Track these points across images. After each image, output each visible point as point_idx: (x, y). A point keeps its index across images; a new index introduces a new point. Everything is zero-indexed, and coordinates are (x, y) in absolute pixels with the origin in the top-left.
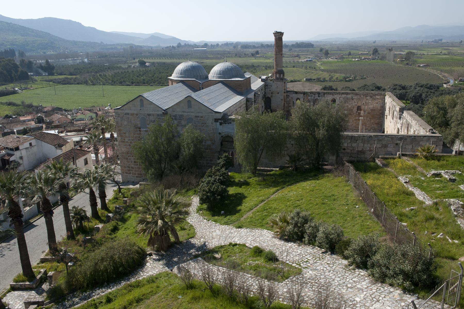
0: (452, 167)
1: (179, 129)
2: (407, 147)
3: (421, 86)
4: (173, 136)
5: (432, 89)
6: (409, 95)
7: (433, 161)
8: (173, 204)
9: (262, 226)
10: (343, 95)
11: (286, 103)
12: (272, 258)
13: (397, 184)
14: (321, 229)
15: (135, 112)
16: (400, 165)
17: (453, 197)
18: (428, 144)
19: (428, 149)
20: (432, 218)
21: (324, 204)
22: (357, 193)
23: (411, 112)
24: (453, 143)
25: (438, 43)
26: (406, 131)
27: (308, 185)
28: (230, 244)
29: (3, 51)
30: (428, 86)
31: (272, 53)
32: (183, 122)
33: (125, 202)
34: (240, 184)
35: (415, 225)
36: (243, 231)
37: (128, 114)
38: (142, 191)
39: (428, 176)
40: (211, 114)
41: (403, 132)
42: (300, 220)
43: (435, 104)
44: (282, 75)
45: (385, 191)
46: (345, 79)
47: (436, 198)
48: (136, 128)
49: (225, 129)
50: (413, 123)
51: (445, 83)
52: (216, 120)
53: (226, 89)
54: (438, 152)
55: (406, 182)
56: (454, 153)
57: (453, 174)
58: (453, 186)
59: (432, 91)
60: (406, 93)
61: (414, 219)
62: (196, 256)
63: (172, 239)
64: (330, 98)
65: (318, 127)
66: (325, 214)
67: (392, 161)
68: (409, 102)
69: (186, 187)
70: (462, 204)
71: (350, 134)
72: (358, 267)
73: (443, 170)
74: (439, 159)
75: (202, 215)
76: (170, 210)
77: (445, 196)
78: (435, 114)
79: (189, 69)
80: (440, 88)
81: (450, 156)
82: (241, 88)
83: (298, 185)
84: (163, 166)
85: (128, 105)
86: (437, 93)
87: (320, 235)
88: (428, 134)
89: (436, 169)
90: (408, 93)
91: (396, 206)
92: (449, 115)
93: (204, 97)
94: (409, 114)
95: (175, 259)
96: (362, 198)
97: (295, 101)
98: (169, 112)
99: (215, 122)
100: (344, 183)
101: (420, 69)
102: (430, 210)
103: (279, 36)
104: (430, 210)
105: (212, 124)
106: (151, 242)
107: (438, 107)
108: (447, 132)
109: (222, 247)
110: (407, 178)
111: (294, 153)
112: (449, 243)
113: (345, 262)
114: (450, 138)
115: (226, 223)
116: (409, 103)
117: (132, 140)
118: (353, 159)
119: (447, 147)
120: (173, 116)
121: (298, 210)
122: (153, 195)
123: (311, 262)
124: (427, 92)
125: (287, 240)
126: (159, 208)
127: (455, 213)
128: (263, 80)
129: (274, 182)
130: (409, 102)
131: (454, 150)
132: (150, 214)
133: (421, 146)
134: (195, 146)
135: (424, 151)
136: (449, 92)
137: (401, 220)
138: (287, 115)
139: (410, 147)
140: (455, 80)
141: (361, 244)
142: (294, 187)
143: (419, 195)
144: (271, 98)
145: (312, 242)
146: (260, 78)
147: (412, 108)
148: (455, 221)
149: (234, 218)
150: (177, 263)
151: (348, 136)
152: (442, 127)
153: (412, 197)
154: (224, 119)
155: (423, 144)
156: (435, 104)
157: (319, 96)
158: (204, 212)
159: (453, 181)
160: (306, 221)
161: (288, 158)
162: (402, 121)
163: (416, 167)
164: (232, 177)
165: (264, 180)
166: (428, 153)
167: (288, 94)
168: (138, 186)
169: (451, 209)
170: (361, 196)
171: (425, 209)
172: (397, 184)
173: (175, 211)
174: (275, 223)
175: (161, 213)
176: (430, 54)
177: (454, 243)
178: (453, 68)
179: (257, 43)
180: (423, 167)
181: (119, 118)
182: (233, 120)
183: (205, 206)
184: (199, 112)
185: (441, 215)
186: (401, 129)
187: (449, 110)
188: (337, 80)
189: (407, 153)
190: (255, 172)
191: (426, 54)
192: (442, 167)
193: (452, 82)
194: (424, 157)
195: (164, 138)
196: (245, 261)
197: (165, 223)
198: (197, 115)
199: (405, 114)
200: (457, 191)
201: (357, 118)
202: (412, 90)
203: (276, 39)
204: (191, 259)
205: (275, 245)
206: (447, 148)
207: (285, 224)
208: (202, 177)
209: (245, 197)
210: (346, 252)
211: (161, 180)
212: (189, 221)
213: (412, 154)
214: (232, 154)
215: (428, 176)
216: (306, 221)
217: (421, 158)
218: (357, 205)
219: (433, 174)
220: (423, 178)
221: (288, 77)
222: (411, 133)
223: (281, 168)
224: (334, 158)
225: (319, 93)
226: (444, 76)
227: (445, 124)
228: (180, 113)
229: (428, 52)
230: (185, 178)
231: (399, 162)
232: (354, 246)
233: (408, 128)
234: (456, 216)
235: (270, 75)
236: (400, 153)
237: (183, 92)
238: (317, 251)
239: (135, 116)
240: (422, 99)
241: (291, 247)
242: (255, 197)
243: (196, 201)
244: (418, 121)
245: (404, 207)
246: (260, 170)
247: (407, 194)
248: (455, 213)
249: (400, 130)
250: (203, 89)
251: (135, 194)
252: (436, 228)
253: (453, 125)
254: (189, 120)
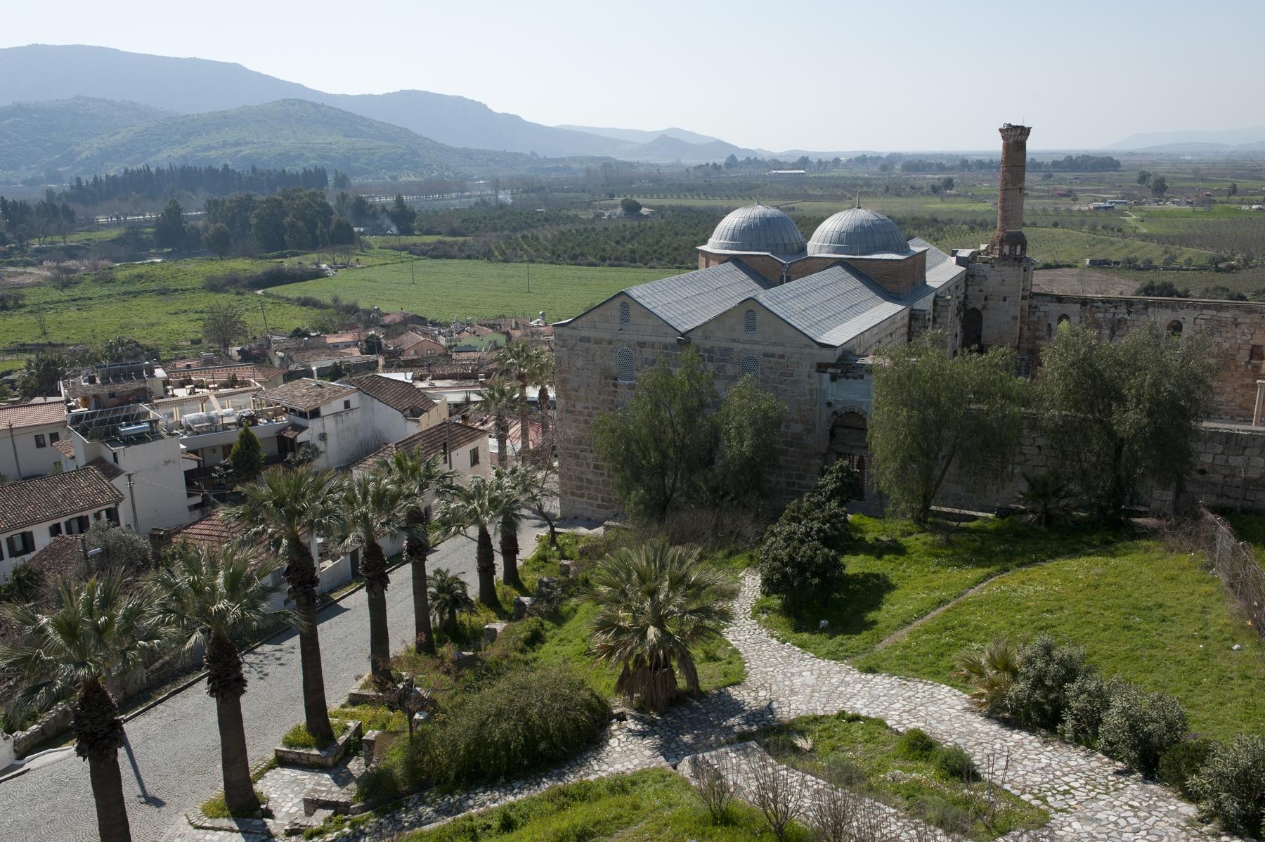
1: (719, 385)
4: (702, 404)
8: (689, 587)
9: (936, 675)
10: (1205, 312)
11: (1025, 328)
12: (961, 769)
14: (1117, 703)
15: (607, 336)
21: (1128, 628)
22: (1237, 605)
27: (1080, 569)
28: (842, 714)
29: (301, 172)
31: (993, 184)
32: (730, 369)
33: (565, 571)
34: (878, 550)
36: (880, 682)
37: (588, 340)
38: (610, 546)
40: (808, 350)
42: (1053, 668)
44: (1019, 248)
46: (1214, 265)
48: (606, 378)
49: (845, 394)
52: (821, 368)
53: (854, 283)
62: (744, 737)
63: (682, 683)
64: (1163, 318)
65: (1122, 400)
66: (1131, 658)
69: (728, 545)
71: (1223, 426)
72: (1231, 830)
75: (766, 624)
76: (679, 600)
79: (756, 225)
82: (897, 282)
83: (1051, 565)
84: (669, 481)
85: (589, 316)
87: (1112, 719)
93: (790, 302)
95: (687, 738)
96: (1254, 621)
97: (1054, 325)
98: (696, 339)
99: (818, 371)
100: (1196, 573)
103: (1015, 137)
105: (809, 376)
106: (625, 684)
109: (816, 719)
111: (1043, 472)
113: (1189, 810)
115: (833, 656)
117: (594, 408)
118: (1230, 503)
120: (705, 351)
121: (1047, 638)
122: (640, 558)
123: (1080, 795)
125: (1010, 724)
126: (652, 593)
128: (960, 261)
129: (977, 552)
132: (628, 608)
134: (758, 433)
138: (1028, 361)
141: (1245, 760)
142: (1036, 572)
144: (984, 313)
145: (1085, 736)
146: (954, 254)
149: (855, 641)
150: (691, 749)
151: (1215, 434)
154: (844, 363)
157: (1129, 313)
158: (774, 617)
160: (1070, 672)
161: (1024, 487)
164: (857, 529)
165: (950, 543)
167: (1035, 302)
168: (600, 531)
170: (1251, 617)
173: (694, 606)
174: (975, 669)
175: (656, 607)
179: (950, 157)
182: (869, 370)
183: (776, 601)
184: (774, 344)
188: (1189, 265)
190: (923, 520)
195: (676, 407)
196: (881, 768)
197: (666, 636)
198: (770, 350)
201: (1249, 381)
203: (1007, 147)
204: (730, 743)
205: (971, 733)
207: (1007, 677)
208: (774, 520)
209: (891, 588)
210: (1192, 781)
211: (661, 520)
212: (730, 638)
214: (861, 464)
216: (1070, 672)
218: (1234, 641)
221: (1036, 254)
223: (1003, 513)
224: (1169, 496)
225: (1129, 303)
228: (725, 344)
230: (727, 520)
232: (1219, 765)
235: (983, 247)
237: (735, 288)
238: (1102, 767)
241: (1019, 745)
242: (921, 588)
243: (751, 584)
246: (938, 514)
250: (789, 280)
251: (592, 552)
254: (748, 364)
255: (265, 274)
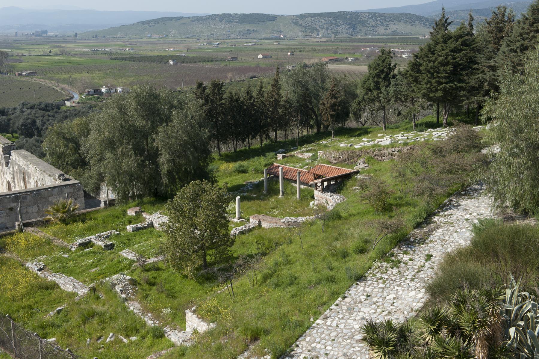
0: (105, 227)
2: (30, 210)
3: (32, 108)
5: (49, 111)
6: (14, 123)
7: (75, 224)
13: (25, 276)
16: (23, 243)
17: (116, 272)
18: (61, 199)
19: (64, 207)
20: (92, 315)
23: (24, 152)
24: (97, 189)
25: (41, 37)
26: (22, 184)
30: (42, 106)
35: (70, 335)
39: (73, 249)
41: (18, 187)
43: (58, 134)
45: (9, 294)
47: (92, 280)
50: (31, 169)
51: (68, 100)
54: (79, 209)
55: (40, 270)
56: (102, 205)
57: (108, 237)
58: (112, 256)
59: (50, 113)
60: (9, 120)
61: (65, 326)
67: (9, 240)
68: (17, 135)
70: (129, 280)
73: (92, 234)
74: (83, 218)
77: (103, 274)
78: (62, 150)
80: (61, 108)
81: (98, 211)
86: (59, 117)
88: (59, 183)
89: (82, 235)
90: (11, 121)
91: (32, 313)
92: (83, 149)
94: (20, 155)
101: (23, 79)
102: (87, 303)
104: (87, 303)
107: (64, 138)
108: (86, 175)
110: (40, 261)
112: (125, 345)
114: (92, 182)
116: (17, 138)
119: (92, 197)
124: (43, 116)
127: (124, 296)
130: (17, 135)
131: (102, 201)
133: (52, 204)
135: (58, 211)
136: (75, 113)
137: (45, 336)
139: (35, 209)
140: (81, 94)
143: (66, 284)
147: (24, 145)
148: (125, 308)
152: (77, 168)
153: (55, 291)
155: (54, 201)
156: (58, 134)
159: (110, 247)
162: (11, 169)
163: (51, 240)
166: (64, 212)
169: (116, 292)
171: (79, 304)
172: (25, 276)
176: (33, 54)
177: (131, 343)
178: (73, 76)
180: (62, 238)
185: (104, 305)
186: (14, 182)
187: (82, 141)
189: (31, 221)
191: (27, 54)
192: (91, 230)
193: (77, 97)
194: (60, 221)
199: (14, 155)
200: (119, 262)
202: (17, 114)
206: (91, 199)
213: (40, 221)
215: (73, 249)
217: (56, 224)
219: (80, 245)
220: (66, 256)
222: (32, 186)
226: (63, 89)
227: (82, 163)
229: (29, 52)
231: (21, 240)
233: (24, 178)
234: (126, 300)
236: (20, 222)
240: (38, 128)
244: (38, 165)
245: (46, 312)
247: (47, 288)
248: (124, 296)
249: (12, 184)
252: (102, 329)
253: (92, 162)
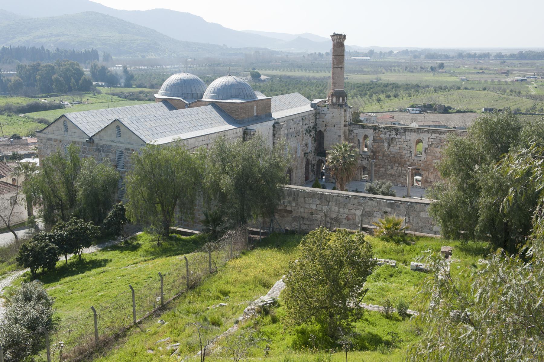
15: (59, 138)
29: (83, 51)
53: (216, 114)
79: (177, 83)
181: (42, 144)
239: (58, 142)
255: (28, 105)
